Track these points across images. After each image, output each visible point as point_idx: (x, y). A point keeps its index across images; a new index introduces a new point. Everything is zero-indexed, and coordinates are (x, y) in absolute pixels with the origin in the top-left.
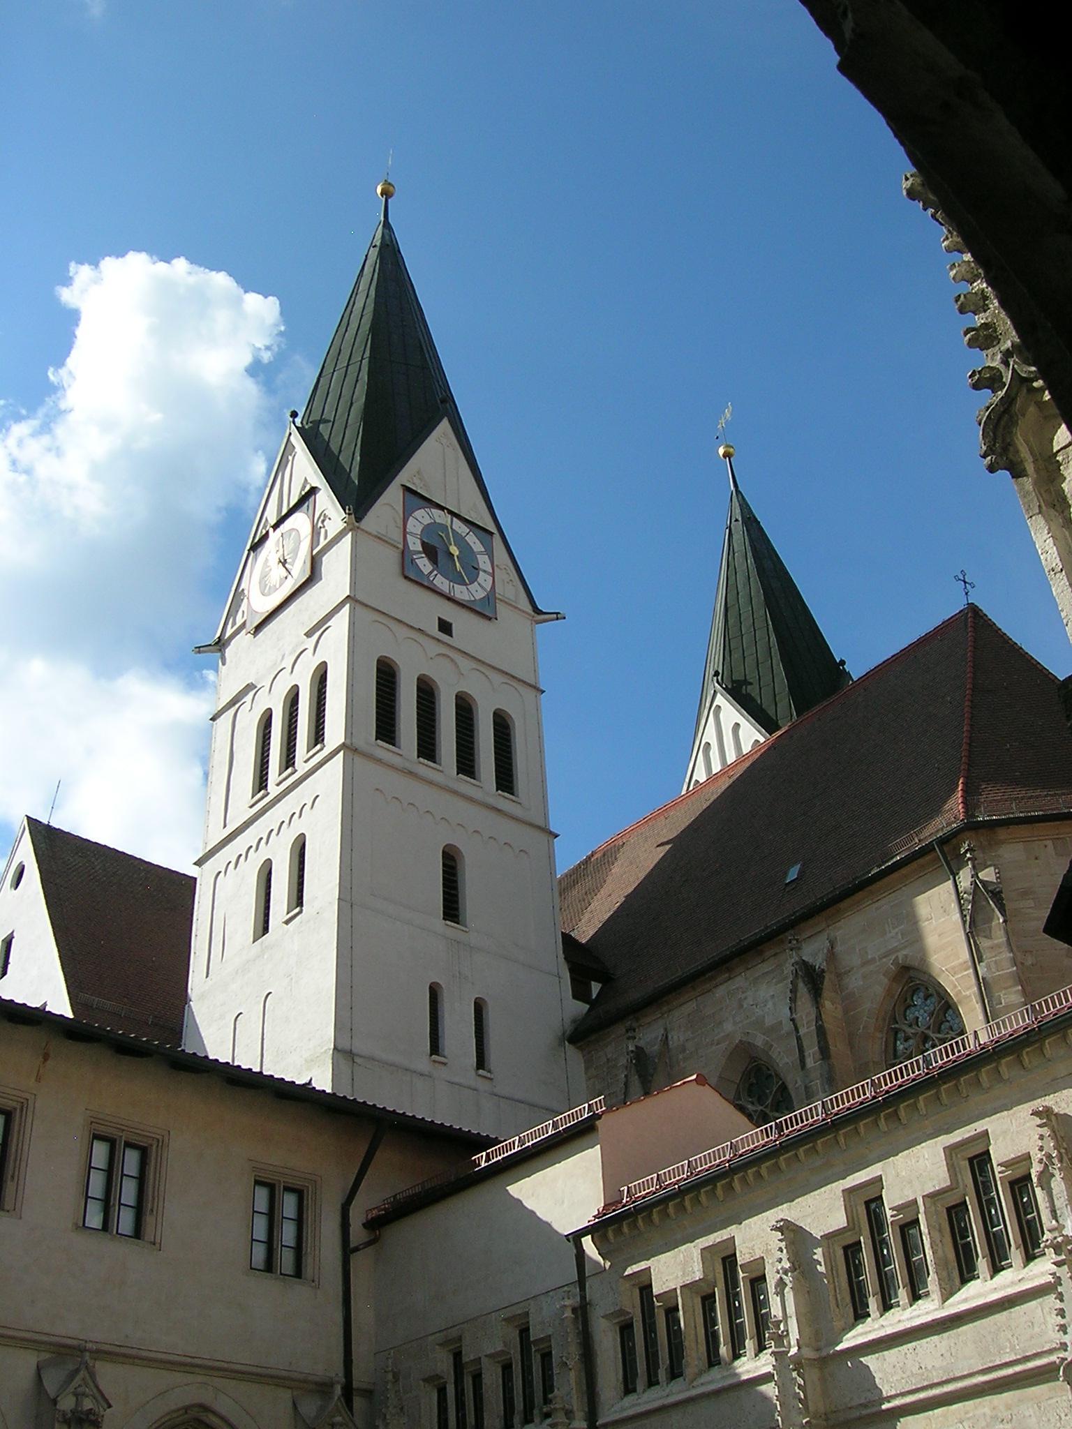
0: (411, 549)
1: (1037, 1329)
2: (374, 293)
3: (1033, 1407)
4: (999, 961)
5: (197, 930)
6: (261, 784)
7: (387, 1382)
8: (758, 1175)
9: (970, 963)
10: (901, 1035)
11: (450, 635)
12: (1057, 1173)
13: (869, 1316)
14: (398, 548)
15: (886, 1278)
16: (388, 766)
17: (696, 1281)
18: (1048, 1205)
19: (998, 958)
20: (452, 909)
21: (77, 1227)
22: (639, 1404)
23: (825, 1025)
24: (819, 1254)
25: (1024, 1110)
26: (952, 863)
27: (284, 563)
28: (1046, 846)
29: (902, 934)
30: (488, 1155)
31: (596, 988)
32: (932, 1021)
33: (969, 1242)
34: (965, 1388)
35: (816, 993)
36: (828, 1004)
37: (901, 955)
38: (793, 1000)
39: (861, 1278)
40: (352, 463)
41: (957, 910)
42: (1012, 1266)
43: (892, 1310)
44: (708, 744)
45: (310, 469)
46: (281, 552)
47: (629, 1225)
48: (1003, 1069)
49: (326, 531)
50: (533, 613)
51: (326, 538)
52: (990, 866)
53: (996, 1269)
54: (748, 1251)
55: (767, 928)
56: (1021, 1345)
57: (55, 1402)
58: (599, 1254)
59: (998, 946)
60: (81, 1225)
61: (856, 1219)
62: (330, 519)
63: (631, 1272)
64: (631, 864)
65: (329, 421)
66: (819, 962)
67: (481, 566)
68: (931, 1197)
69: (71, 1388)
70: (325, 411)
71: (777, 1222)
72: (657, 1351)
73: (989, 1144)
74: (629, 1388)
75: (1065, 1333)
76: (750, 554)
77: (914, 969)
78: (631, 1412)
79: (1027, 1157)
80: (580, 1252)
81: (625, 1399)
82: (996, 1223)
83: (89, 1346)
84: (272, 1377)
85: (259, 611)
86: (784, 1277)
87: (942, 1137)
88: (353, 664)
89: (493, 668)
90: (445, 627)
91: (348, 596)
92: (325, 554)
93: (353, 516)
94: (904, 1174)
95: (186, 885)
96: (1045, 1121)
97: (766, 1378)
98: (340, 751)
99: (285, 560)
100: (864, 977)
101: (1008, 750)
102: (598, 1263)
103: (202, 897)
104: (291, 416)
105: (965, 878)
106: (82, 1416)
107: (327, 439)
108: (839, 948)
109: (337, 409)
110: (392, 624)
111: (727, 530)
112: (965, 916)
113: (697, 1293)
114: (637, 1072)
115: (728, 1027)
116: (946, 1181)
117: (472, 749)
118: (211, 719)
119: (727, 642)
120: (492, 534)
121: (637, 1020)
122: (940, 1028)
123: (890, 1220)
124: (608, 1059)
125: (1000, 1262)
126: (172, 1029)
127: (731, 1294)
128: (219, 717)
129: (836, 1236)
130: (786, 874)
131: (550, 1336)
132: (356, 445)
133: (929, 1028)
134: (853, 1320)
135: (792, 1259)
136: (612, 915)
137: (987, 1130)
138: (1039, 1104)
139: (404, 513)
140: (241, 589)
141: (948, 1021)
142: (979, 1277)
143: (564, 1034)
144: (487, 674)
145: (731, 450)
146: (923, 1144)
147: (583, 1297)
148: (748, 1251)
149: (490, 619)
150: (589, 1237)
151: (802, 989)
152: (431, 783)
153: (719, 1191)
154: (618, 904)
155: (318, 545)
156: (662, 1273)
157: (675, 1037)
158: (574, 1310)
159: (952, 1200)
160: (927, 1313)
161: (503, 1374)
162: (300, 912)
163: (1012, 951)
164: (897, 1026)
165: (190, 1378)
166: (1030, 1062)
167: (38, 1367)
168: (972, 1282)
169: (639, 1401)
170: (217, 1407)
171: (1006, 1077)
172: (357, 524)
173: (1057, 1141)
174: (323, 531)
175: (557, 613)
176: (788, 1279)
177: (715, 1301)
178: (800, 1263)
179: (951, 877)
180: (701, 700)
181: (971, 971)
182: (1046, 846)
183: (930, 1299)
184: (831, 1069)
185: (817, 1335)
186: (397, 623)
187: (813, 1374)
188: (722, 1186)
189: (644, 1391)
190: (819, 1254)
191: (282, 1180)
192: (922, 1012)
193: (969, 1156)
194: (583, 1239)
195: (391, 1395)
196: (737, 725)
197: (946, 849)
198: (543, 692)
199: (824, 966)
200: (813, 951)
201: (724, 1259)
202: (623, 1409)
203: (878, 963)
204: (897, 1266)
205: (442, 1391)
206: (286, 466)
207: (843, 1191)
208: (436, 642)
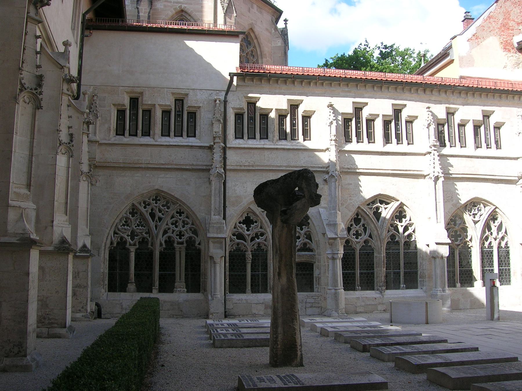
37: (183, 6)
78: (246, 146)
82: (399, 130)
100: (165, 6)
131: (200, 107)
147: (225, 98)
202: (239, 144)
203: (172, 4)
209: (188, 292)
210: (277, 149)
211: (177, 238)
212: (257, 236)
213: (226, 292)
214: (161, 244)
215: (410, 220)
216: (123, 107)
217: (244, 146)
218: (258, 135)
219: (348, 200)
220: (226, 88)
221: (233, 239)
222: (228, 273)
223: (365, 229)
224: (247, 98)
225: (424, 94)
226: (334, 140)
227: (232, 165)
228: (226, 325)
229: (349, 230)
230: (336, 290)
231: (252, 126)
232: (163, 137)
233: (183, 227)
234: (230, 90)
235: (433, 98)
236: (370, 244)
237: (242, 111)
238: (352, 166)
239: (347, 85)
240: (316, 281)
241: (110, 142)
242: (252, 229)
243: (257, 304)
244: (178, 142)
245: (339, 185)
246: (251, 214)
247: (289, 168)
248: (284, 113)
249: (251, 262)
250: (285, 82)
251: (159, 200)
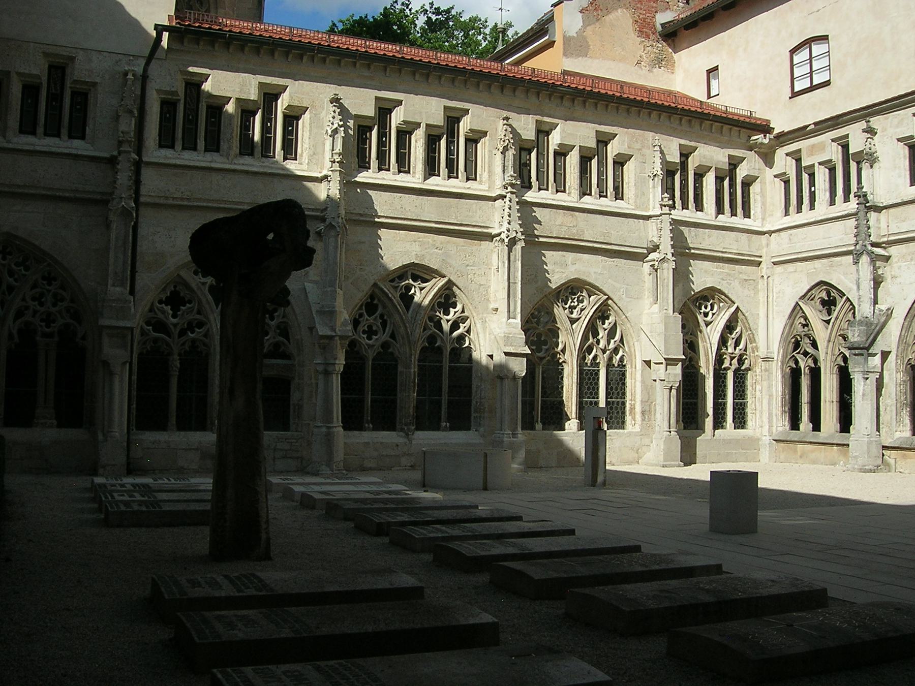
78: (178, 162)
116: (441, 123)
131: (97, 83)
202: (166, 157)
209: (60, 426)
210: (234, 171)
211: (41, 326)
212: (191, 327)
213: (131, 428)
214: (11, 336)
215: (463, 312)
217: (174, 162)
218: (201, 144)
220: (147, 53)
221: (147, 331)
222: (134, 393)
223: (384, 324)
224: (186, 75)
225: (500, 94)
226: (338, 162)
227: (150, 196)
228: (129, 487)
229: (356, 323)
230: (329, 428)
231: (191, 127)
232: (23, 135)
233: (54, 305)
236: (390, 350)
237: (174, 98)
238: (366, 210)
239: (369, 66)
240: (294, 411)
242: (183, 314)
243: (185, 450)
244: (51, 146)
245: (343, 243)
246: (181, 288)
248: (251, 107)
249: (177, 373)
250: (257, 51)
251: (10, 253)
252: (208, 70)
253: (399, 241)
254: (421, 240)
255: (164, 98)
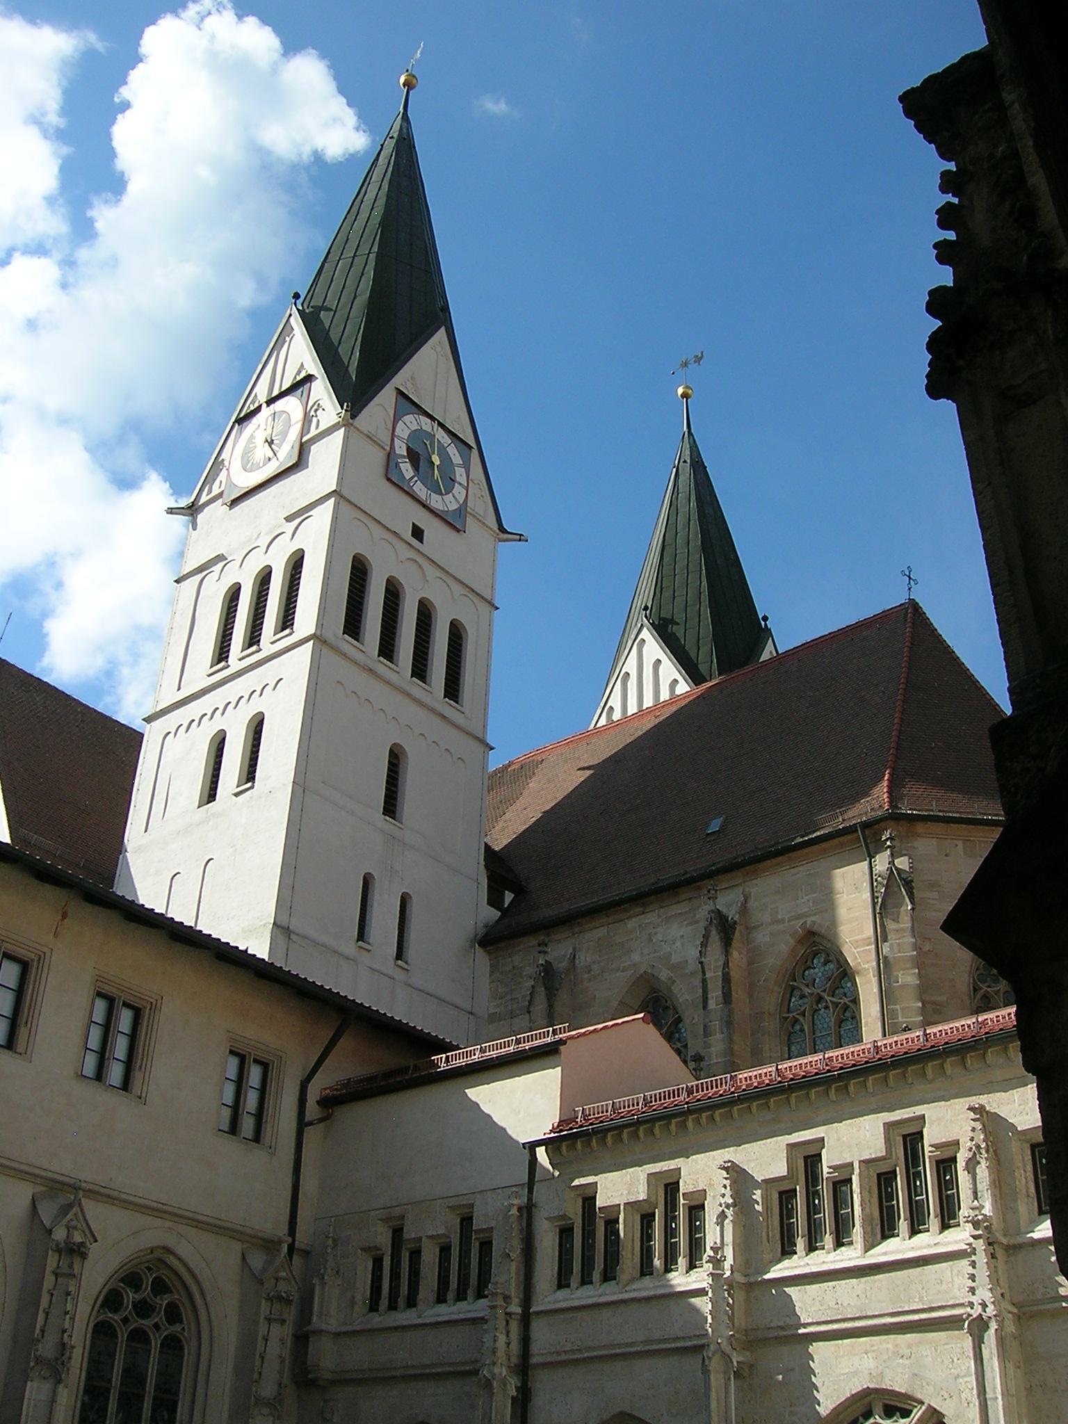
0: (397, 452)
1: (944, 1287)
2: (387, 186)
3: (930, 1349)
4: (901, 944)
5: (139, 784)
6: (220, 654)
7: (327, 1247)
8: (712, 1118)
9: (873, 940)
10: (797, 993)
11: (421, 541)
12: (983, 1162)
13: (796, 1253)
14: (384, 449)
15: (815, 1223)
16: (352, 661)
17: (639, 1201)
18: (971, 1186)
19: (901, 941)
20: (391, 807)
21: (78, 1076)
22: (573, 1299)
23: (731, 973)
24: (757, 1195)
25: (961, 1104)
26: (870, 846)
27: (270, 443)
28: (957, 845)
29: (813, 902)
30: (447, 1057)
31: (509, 897)
32: (828, 985)
33: (893, 1205)
34: (875, 1326)
35: (727, 942)
36: (735, 954)
38: (704, 945)
39: (792, 1221)
40: (350, 358)
41: (869, 889)
42: (929, 1231)
43: (817, 1252)
44: (627, 674)
45: (309, 355)
46: (269, 431)
47: (582, 1142)
48: (948, 1067)
49: (318, 421)
50: (498, 531)
51: (317, 428)
52: (905, 855)
53: (914, 1231)
54: (692, 1182)
55: (686, 873)
56: (929, 1298)
57: (50, 1232)
58: (550, 1163)
59: (903, 930)
60: (80, 1073)
61: (795, 1169)
62: (323, 410)
63: (578, 1184)
64: (549, 782)
65: (332, 310)
66: (732, 913)
67: (458, 478)
68: (866, 1163)
69: (65, 1222)
70: (327, 299)
71: (725, 1162)
72: (594, 1256)
73: (923, 1127)
74: (562, 1282)
75: (974, 1294)
76: (693, 498)
77: (819, 935)
78: (564, 1305)
79: (957, 1143)
80: (533, 1160)
81: (559, 1292)
83: (84, 1185)
84: (228, 1229)
85: (239, 485)
86: (726, 1210)
87: (883, 1114)
88: (331, 558)
89: (456, 579)
90: (418, 533)
91: (335, 491)
92: (314, 443)
93: (349, 413)
94: (845, 1139)
95: (133, 740)
96: (978, 1116)
97: (701, 1292)
98: (310, 640)
99: (272, 441)
101: (932, 748)
102: (549, 1171)
103: (148, 754)
104: (293, 297)
105: (882, 862)
106: (75, 1247)
107: (327, 328)
108: (750, 904)
109: (339, 299)
110: (372, 524)
111: (675, 469)
112: (877, 898)
113: (638, 1211)
114: (544, 984)
115: (636, 957)
117: (427, 654)
118: (175, 581)
119: (660, 579)
120: (470, 448)
121: (548, 935)
122: (834, 992)
123: (825, 1175)
124: (514, 967)
125: (919, 1226)
126: (100, 874)
127: (670, 1216)
128: (185, 580)
129: (774, 1182)
130: (707, 825)
131: (492, 1228)
132: (356, 340)
133: (825, 991)
134: (780, 1256)
135: (733, 1196)
136: (527, 829)
137: (924, 1115)
138: (976, 1101)
139: (394, 418)
140: (220, 459)
141: (842, 988)
142: (898, 1236)
143: (476, 936)
144: (448, 582)
145: (690, 391)
146: (866, 1117)
147: (530, 1199)
148: (692, 1182)
149: (458, 531)
150: (544, 1148)
151: (715, 936)
152: (388, 682)
153: (673, 1127)
154: (534, 819)
155: (308, 432)
156: (608, 1189)
157: (583, 958)
158: (520, 1209)
159: (884, 1168)
160: (850, 1259)
161: (440, 1255)
162: (252, 787)
163: (914, 937)
164: (795, 984)
165: (158, 1222)
166: (972, 1064)
167: (33, 1197)
168: (892, 1239)
169: (573, 1296)
170: (179, 1251)
171: (949, 1072)
172: (351, 421)
173: (986, 1136)
174: (315, 420)
175: (521, 535)
176: (729, 1212)
177: (655, 1220)
178: (741, 1201)
179: (868, 859)
180: (625, 629)
181: (873, 946)
182: (957, 845)
183: (852, 1247)
184: (730, 1013)
185: (747, 1263)
186: (375, 523)
187: (740, 1295)
188: (676, 1123)
189: (577, 1288)
190: (757, 1195)
191: (253, 1052)
192: (819, 971)
193: (904, 1133)
194: (537, 1149)
195: (330, 1258)
196: (659, 661)
197: (867, 832)
198: (498, 608)
199: (737, 917)
200: (727, 901)
201: (666, 1186)
202: (557, 1301)
203: (786, 924)
204: (827, 1215)
205: (378, 1262)
206: (282, 346)
207: (787, 1145)
208: (408, 547)
210: (623, 1302)
216: (378, 1252)
219: (787, 1416)
220: (525, 1178)
227: (542, 1354)
234: (536, 1179)
235: (998, 1075)
238: (788, 1318)
241: (349, 1328)
247: (615, 1349)
250: (635, 1135)
252: (594, 1177)
253: (842, 1356)
254: (875, 1348)
255: (563, 1225)
